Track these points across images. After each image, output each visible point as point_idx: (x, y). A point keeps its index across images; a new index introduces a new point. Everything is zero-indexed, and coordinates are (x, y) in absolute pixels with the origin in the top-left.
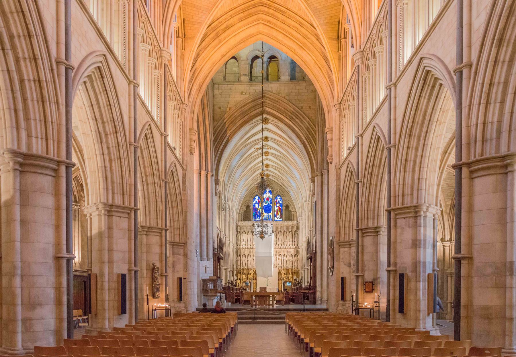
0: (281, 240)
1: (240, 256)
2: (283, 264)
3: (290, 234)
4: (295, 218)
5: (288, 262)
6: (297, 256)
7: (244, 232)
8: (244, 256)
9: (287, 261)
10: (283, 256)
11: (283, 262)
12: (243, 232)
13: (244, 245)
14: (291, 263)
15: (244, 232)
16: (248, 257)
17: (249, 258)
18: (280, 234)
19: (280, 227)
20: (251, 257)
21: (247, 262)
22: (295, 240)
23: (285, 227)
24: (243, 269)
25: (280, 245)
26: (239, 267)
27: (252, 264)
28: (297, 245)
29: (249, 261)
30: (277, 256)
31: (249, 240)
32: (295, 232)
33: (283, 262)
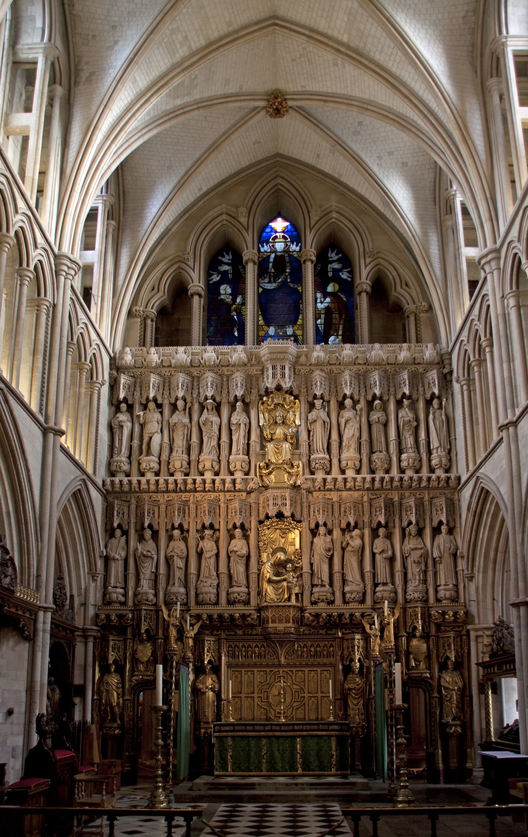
0: (354, 445)
1: (125, 533)
2: (368, 577)
3: (406, 414)
4: (425, 333)
5: (398, 565)
6: (451, 531)
7: (152, 405)
8: (148, 533)
9: (392, 560)
10: (367, 532)
11: (368, 567)
12: (145, 407)
13: (150, 476)
14: (413, 570)
15: (152, 405)
16: (171, 538)
17: (178, 546)
18: (347, 414)
19: (347, 376)
20: (185, 540)
21: (162, 570)
22: (435, 443)
23: (375, 377)
24: (137, 609)
25: (350, 473)
26: (117, 594)
27: (193, 578)
28: (447, 471)
29: (179, 563)
30: (337, 533)
31: (180, 442)
32: (429, 403)
33: (368, 567)
